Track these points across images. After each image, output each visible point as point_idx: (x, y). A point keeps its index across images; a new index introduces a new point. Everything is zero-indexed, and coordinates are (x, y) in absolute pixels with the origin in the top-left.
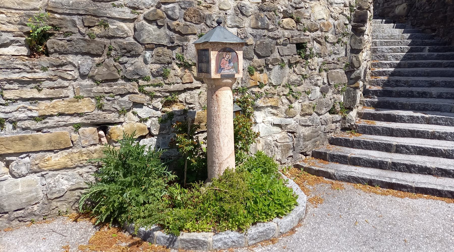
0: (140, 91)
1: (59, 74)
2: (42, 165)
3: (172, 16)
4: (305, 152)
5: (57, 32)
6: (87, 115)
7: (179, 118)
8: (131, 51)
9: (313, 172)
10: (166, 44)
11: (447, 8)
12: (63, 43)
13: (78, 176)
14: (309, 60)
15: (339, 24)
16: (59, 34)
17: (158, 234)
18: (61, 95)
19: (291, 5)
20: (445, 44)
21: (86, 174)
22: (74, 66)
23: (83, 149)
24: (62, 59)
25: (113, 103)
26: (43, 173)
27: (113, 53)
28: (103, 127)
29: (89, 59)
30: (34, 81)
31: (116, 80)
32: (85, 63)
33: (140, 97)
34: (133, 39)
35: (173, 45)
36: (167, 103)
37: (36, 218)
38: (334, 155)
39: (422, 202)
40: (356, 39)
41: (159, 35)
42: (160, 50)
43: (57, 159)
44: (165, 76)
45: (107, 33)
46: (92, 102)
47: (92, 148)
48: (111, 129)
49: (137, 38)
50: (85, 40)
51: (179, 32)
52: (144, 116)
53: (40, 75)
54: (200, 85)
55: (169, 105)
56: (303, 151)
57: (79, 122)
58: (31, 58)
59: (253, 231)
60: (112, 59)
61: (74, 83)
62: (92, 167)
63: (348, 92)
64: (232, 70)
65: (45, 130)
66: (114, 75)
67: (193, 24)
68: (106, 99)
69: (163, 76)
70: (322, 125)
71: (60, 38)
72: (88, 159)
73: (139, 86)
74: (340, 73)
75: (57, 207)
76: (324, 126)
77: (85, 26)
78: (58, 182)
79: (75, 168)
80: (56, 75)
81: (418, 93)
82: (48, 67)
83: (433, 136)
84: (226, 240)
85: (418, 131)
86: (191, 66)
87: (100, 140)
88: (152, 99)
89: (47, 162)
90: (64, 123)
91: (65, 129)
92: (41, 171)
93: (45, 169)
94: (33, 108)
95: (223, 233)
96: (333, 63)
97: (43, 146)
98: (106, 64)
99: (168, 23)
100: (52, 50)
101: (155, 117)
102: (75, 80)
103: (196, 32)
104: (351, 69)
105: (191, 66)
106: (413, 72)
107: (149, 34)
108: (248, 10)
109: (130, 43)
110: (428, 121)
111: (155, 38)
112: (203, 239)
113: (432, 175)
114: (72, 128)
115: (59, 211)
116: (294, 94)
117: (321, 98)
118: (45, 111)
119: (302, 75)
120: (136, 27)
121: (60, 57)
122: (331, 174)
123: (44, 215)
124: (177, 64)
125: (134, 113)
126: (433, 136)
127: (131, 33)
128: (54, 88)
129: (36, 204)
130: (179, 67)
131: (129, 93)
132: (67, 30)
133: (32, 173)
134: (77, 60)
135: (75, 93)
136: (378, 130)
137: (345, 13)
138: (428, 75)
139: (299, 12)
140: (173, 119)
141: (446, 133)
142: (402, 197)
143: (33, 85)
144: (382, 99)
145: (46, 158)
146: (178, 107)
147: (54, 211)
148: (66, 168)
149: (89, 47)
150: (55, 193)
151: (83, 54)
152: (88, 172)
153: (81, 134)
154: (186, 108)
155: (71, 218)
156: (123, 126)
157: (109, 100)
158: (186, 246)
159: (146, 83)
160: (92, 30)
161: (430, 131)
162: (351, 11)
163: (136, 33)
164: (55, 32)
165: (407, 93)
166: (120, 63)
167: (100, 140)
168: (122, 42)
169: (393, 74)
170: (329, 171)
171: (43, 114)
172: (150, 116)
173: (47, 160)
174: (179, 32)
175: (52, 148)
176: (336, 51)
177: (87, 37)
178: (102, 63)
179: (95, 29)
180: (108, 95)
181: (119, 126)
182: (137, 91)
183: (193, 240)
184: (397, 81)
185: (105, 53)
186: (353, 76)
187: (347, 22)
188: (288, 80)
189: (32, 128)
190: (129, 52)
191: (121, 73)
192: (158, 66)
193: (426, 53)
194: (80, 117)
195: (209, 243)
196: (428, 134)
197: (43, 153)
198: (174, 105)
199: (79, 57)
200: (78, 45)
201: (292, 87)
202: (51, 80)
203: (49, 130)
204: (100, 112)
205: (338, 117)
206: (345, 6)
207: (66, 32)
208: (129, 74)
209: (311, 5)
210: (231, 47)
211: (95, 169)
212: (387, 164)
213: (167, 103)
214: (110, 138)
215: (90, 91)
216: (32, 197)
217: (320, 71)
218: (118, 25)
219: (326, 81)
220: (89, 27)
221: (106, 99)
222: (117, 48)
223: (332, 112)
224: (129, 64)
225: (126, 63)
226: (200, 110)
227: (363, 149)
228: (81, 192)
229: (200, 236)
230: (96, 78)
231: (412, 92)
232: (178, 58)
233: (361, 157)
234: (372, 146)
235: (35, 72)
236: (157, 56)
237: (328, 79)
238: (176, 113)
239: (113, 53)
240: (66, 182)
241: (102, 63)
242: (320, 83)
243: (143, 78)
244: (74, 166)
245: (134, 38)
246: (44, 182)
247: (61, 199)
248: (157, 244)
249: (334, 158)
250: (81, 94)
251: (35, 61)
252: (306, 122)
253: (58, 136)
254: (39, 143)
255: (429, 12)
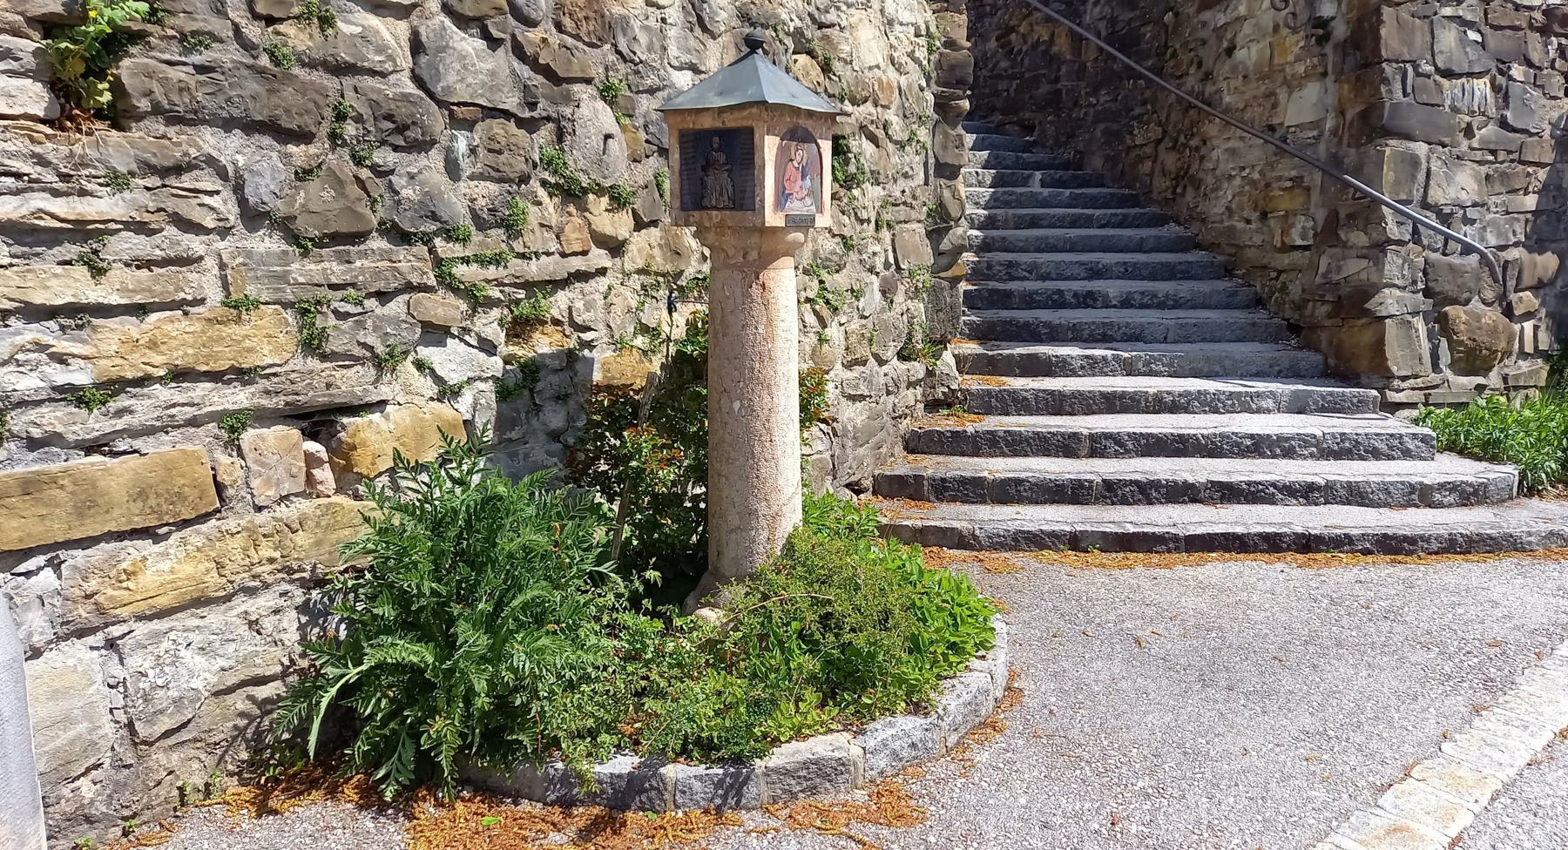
0: (440, 277)
1: (171, 205)
2: (111, 598)
3: (526, 10)
4: (858, 483)
5: (159, 28)
6: (267, 376)
7: (555, 379)
8: (407, 127)
9: (907, 535)
10: (514, 110)
11: (1059, 69)
12: (183, 76)
13: (243, 630)
14: (856, 192)
15: (910, 86)
16: (162, 38)
17: (674, 771)
18: (182, 295)
19: (810, 14)
20: (1066, 166)
21: (273, 618)
22: (222, 174)
23: (264, 517)
24: (179, 144)
25: (360, 325)
26: (116, 631)
27: (350, 129)
28: (318, 421)
29: (272, 149)
30: (81, 231)
31: (358, 237)
32: (266, 167)
33: (443, 304)
34: (410, 83)
35: (535, 114)
36: (519, 328)
37: (92, 835)
38: (943, 480)
39: (1217, 569)
40: (946, 135)
41: (492, 74)
42: (497, 127)
43: (165, 566)
44: (511, 228)
45: (333, 51)
46: (287, 324)
47: (282, 511)
48: (350, 429)
49: (426, 78)
50: (261, 72)
51: (547, 72)
52: (453, 378)
53: (103, 206)
54: (607, 263)
55: (518, 336)
56: (853, 479)
57: (246, 404)
58: (63, 129)
59: (952, 700)
60: (345, 153)
61: (221, 245)
62: (288, 587)
63: (934, 291)
64: (808, 201)
65: (122, 446)
66: (361, 217)
67: (580, 45)
68: (335, 312)
69: (508, 227)
70: (888, 393)
71: (167, 57)
72: (277, 555)
73: (438, 262)
74: (916, 232)
75: (170, 773)
76: (892, 397)
77: (256, 16)
78: (173, 663)
79: (228, 598)
80: (160, 210)
81: (1075, 295)
82: (132, 174)
83: (1160, 405)
84: (897, 745)
85: (1123, 395)
86: (585, 191)
87: (310, 480)
88: (475, 311)
89: (131, 584)
90: (190, 412)
91: (190, 439)
92: (107, 625)
93: (124, 612)
94: (76, 351)
95: (877, 725)
96: (904, 203)
97: (116, 512)
98: (332, 173)
99: (517, 32)
100: (144, 104)
101: (486, 380)
102: (224, 232)
103: (593, 73)
104: (939, 223)
105: (585, 191)
106: (1037, 239)
107: (465, 67)
108: (716, 14)
109: (405, 97)
110: (1130, 369)
111: (483, 84)
112: (837, 754)
113: (1201, 502)
114: (216, 431)
115: (181, 789)
116: (830, 296)
117: (883, 310)
118: (121, 361)
119: (843, 237)
120: (424, 39)
121: (172, 131)
122: (965, 533)
123: (126, 813)
124: (544, 183)
125: (420, 365)
126: (1160, 405)
127: (405, 61)
128: (148, 264)
129: (88, 770)
130: (551, 195)
131: (409, 288)
132: (195, 26)
133: (66, 638)
134: (231, 148)
135: (225, 286)
136: (1025, 399)
137: (917, 54)
138: (1072, 247)
139: (826, 38)
140: (540, 386)
141: (1187, 394)
142: (1167, 566)
143: (71, 250)
144: (991, 314)
145: (124, 565)
146: (546, 340)
147: (162, 791)
148: (201, 602)
149: (275, 100)
150: (161, 712)
151: (251, 127)
152: (276, 612)
153: (250, 456)
154: (572, 343)
155: (240, 808)
156: (387, 418)
157: (346, 315)
158: (784, 791)
159: (457, 250)
160: (278, 33)
161: (1151, 391)
162: (930, 51)
163: (423, 59)
164: (149, 27)
165: (1050, 297)
166: (374, 168)
167: (310, 480)
168: (379, 91)
169: (984, 247)
170: (956, 524)
171: (114, 373)
172: (471, 375)
173: (130, 574)
174: (547, 72)
175: (151, 521)
176: (907, 169)
177: (264, 60)
178: (319, 166)
179: (287, 28)
180: (340, 294)
181: (376, 417)
182: (432, 282)
183: (805, 765)
184: (1010, 264)
185: (324, 130)
186: (945, 245)
187: (924, 84)
188: (815, 254)
189: (71, 437)
190: (401, 129)
191: (381, 212)
192: (493, 188)
193: (1035, 187)
194: (245, 384)
195: (855, 764)
196: (1147, 400)
197: (113, 545)
198: (537, 335)
199: (236, 139)
200: (239, 92)
201: (825, 275)
202: (141, 228)
203: (138, 443)
204: (313, 363)
205: (918, 369)
206: (917, 35)
207: (194, 33)
208: (408, 214)
209: (852, 20)
210: (808, 124)
211: (299, 596)
212: (1091, 488)
213: (519, 328)
214: (348, 468)
215: (283, 278)
216: (73, 742)
217: (878, 228)
218: (365, 23)
219: (892, 260)
220: (270, 20)
221: (335, 312)
222: (366, 112)
223: (903, 356)
224: (400, 176)
225: (392, 172)
226: (609, 353)
227: (1004, 455)
228: (251, 698)
229: (821, 746)
230: (301, 225)
231: (1060, 292)
232: (548, 163)
233: (1023, 475)
234: (1029, 444)
235: (83, 193)
236: (490, 151)
237: (894, 251)
238: (548, 361)
239: (350, 129)
240: (200, 661)
241: (319, 166)
242: (879, 264)
243: (450, 234)
244: (230, 589)
245: (417, 80)
246: (119, 672)
247: (185, 735)
248: (677, 807)
249: (946, 489)
250: (251, 290)
251: (82, 145)
252: (856, 387)
253: (170, 467)
254: (100, 501)
255: (1013, 77)
